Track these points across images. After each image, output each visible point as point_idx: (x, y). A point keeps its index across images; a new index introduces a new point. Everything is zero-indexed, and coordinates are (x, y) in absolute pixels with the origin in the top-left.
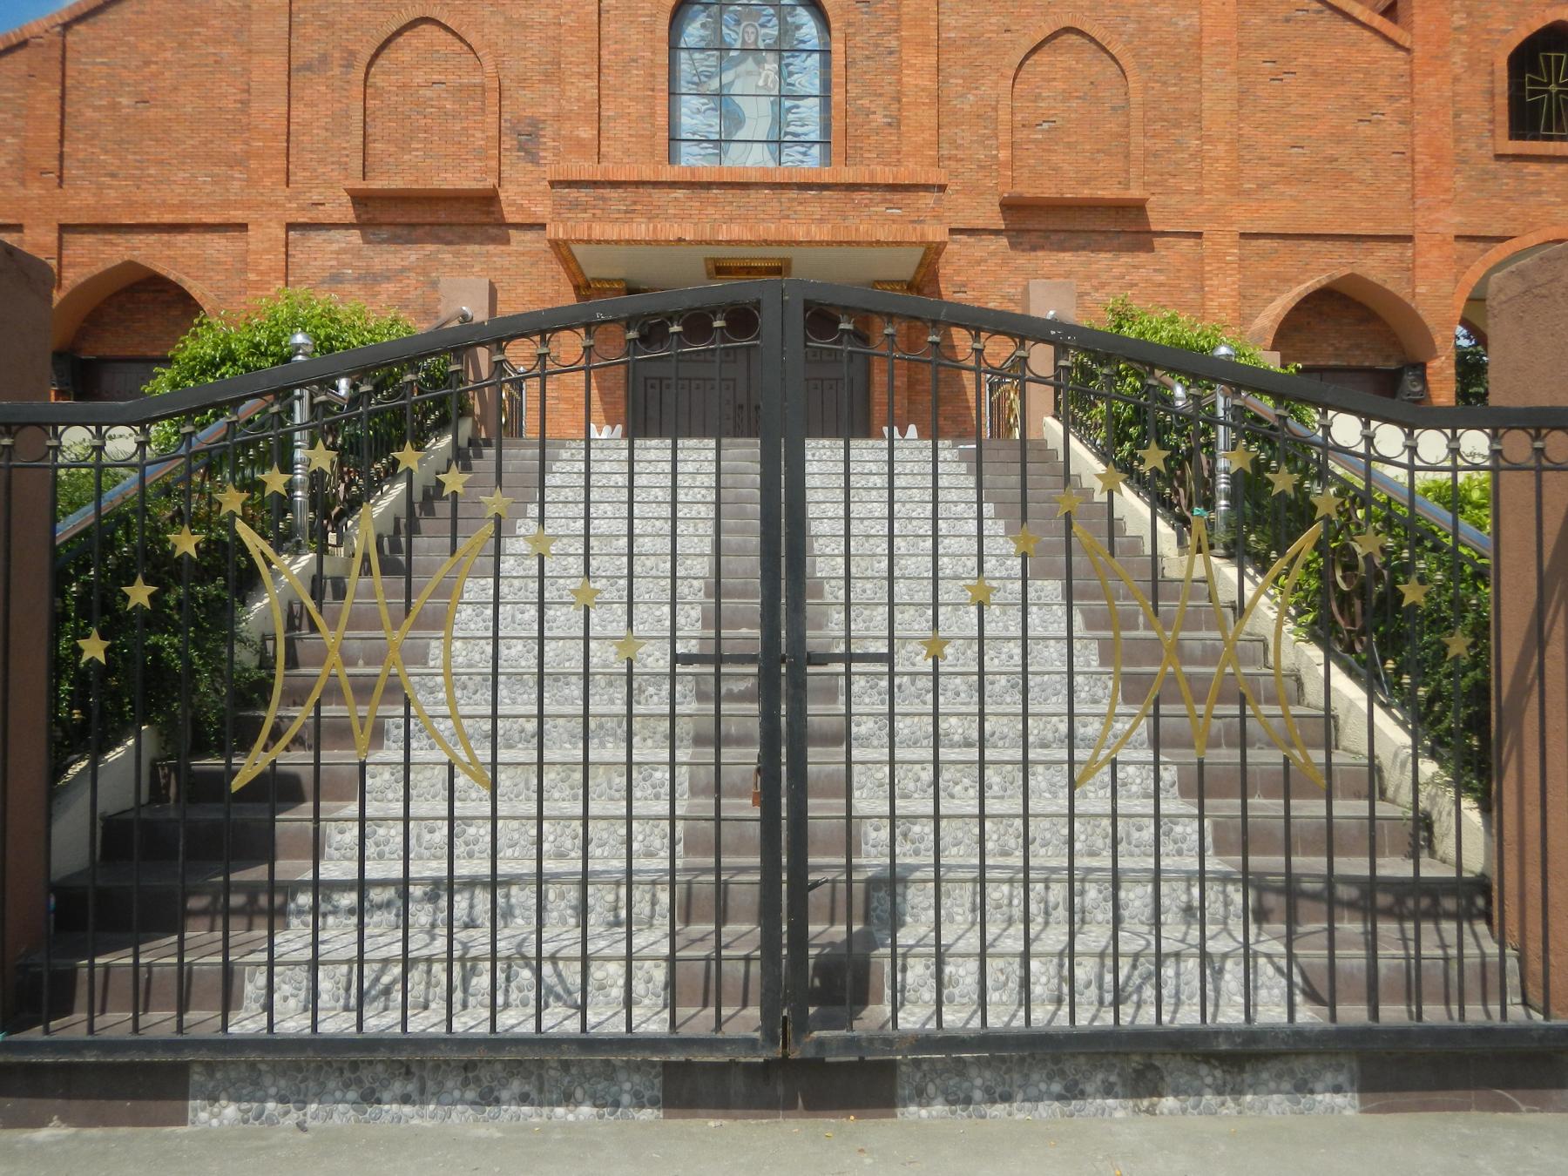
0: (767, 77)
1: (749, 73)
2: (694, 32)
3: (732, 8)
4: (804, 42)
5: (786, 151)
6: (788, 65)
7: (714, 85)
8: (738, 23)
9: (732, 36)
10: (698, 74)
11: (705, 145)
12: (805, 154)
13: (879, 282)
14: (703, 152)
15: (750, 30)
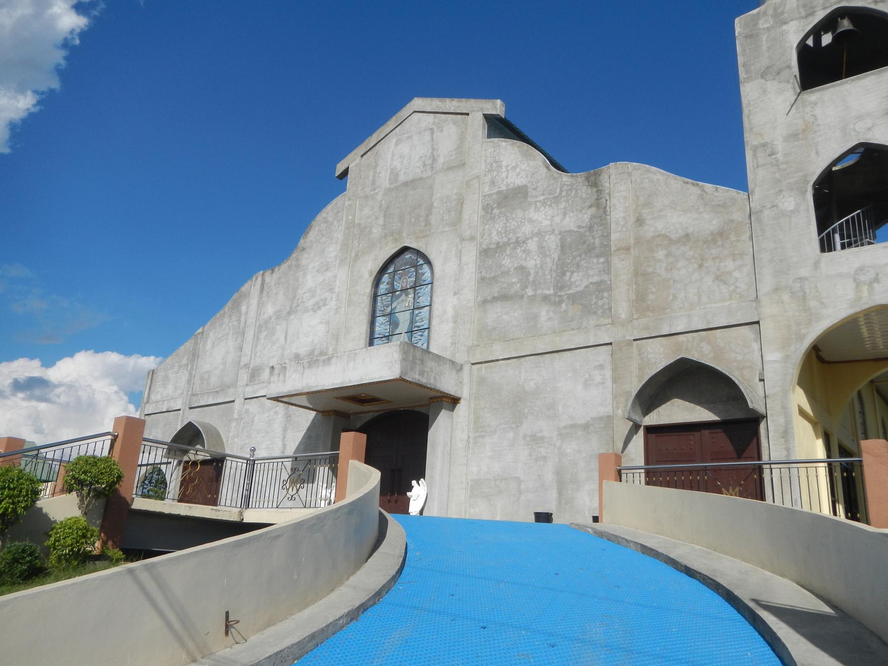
0: (410, 301)
1: (403, 301)
2: (383, 287)
3: (398, 272)
4: (425, 281)
5: (415, 335)
6: (418, 293)
7: (389, 310)
8: (400, 278)
9: (398, 286)
10: (384, 306)
11: (383, 339)
12: (421, 336)
13: (431, 398)
14: (382, 342)
15: (405, 280)
